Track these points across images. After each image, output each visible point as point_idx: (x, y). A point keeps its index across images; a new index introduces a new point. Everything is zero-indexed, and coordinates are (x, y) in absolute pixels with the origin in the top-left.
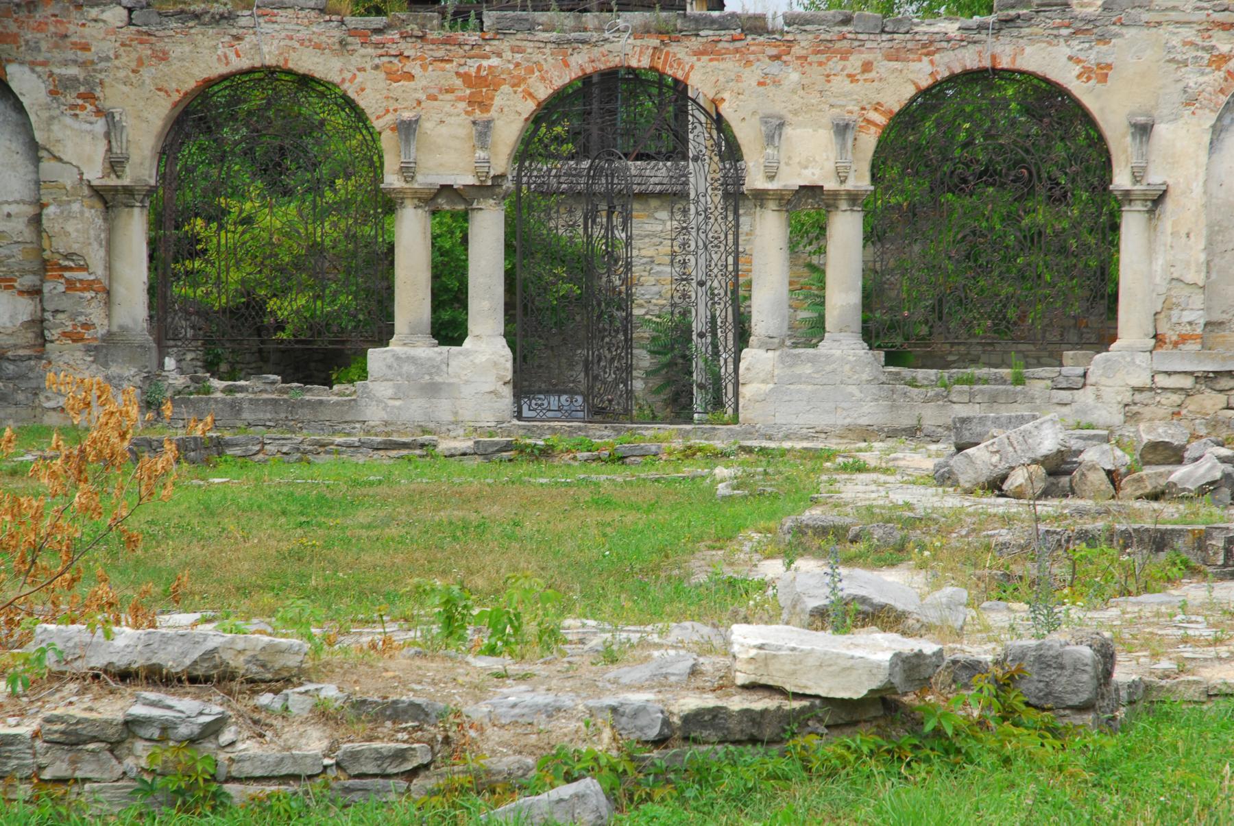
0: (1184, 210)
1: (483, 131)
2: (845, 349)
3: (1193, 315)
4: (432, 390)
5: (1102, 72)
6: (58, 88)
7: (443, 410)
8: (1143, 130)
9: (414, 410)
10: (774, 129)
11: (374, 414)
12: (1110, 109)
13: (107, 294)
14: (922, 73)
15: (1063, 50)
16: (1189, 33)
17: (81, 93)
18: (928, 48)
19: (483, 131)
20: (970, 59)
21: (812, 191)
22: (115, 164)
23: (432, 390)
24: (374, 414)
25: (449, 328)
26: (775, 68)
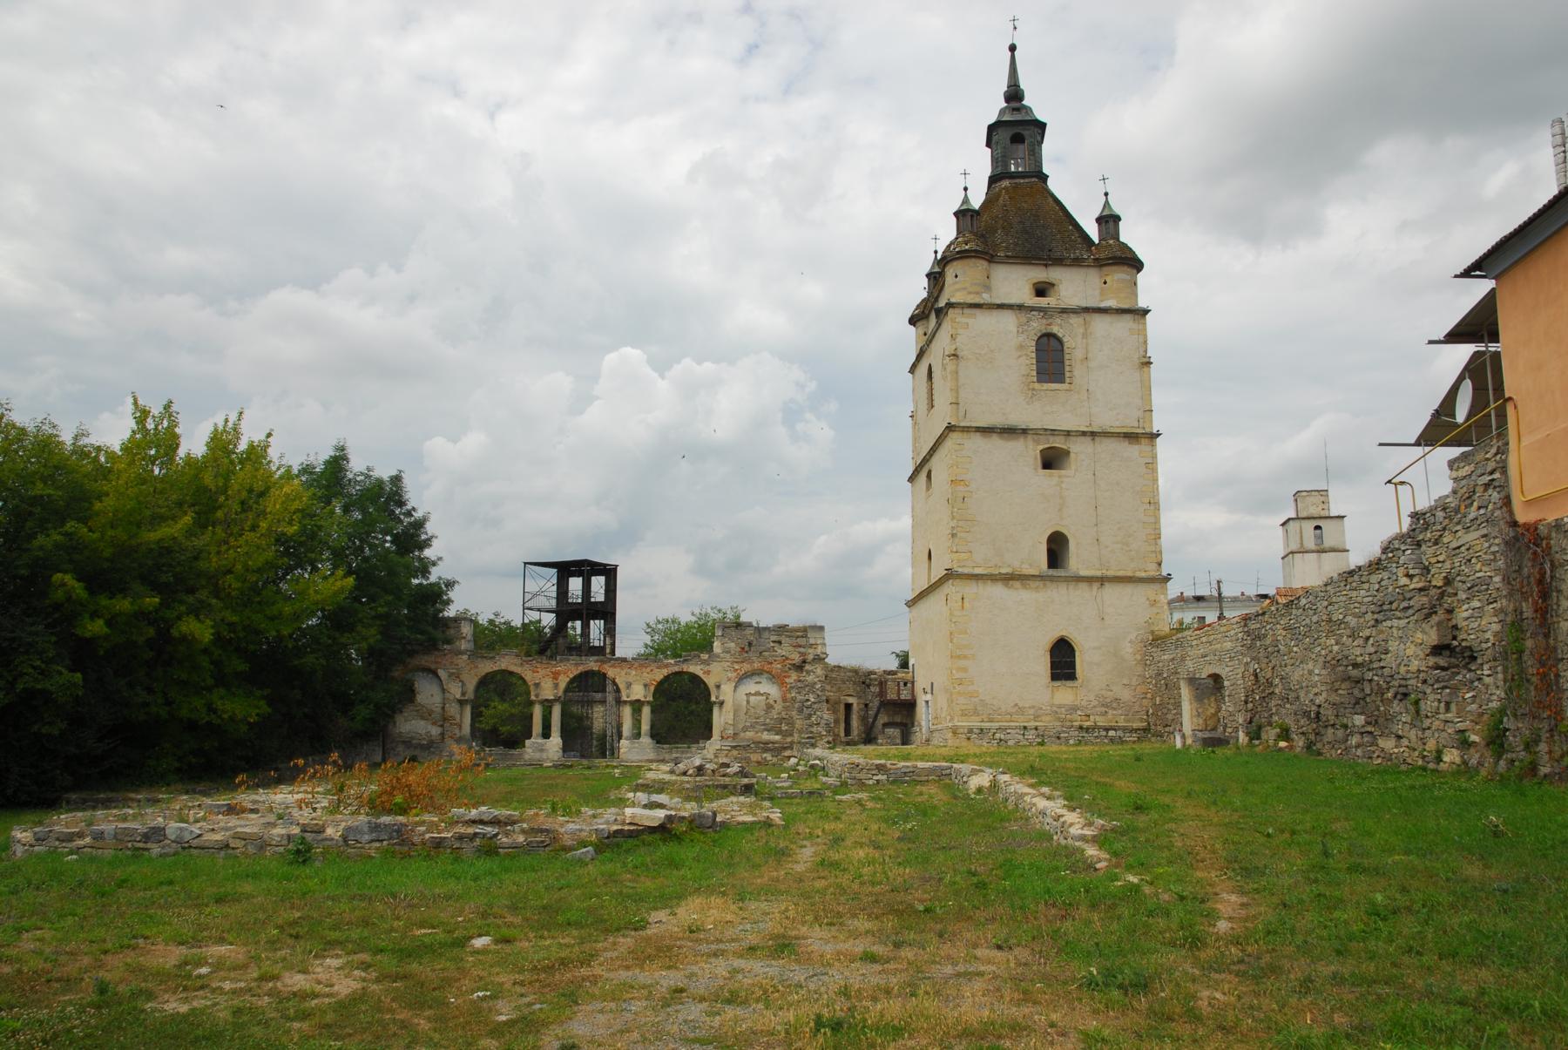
0: (728, 706)
1: (556, 686)
2: (646, 740)
3: (731, 732)
4: (542, 750)
5: (708, 672)
6: (451, 675)
7: (544, 756)
8: (718, 687)
9: (538, 755)
10: (629, 685)
11: (527, 757)
12: (710, 681)
13: (460, 727)
14: (665, 672)
17: (456, 676)
18: (667, 666)
19: (556, 686)
20: (676, 669)
21: (638, 701)
22: (463, 694)
23: (542, 750)
24: (527, 757)
25: (546, 734)
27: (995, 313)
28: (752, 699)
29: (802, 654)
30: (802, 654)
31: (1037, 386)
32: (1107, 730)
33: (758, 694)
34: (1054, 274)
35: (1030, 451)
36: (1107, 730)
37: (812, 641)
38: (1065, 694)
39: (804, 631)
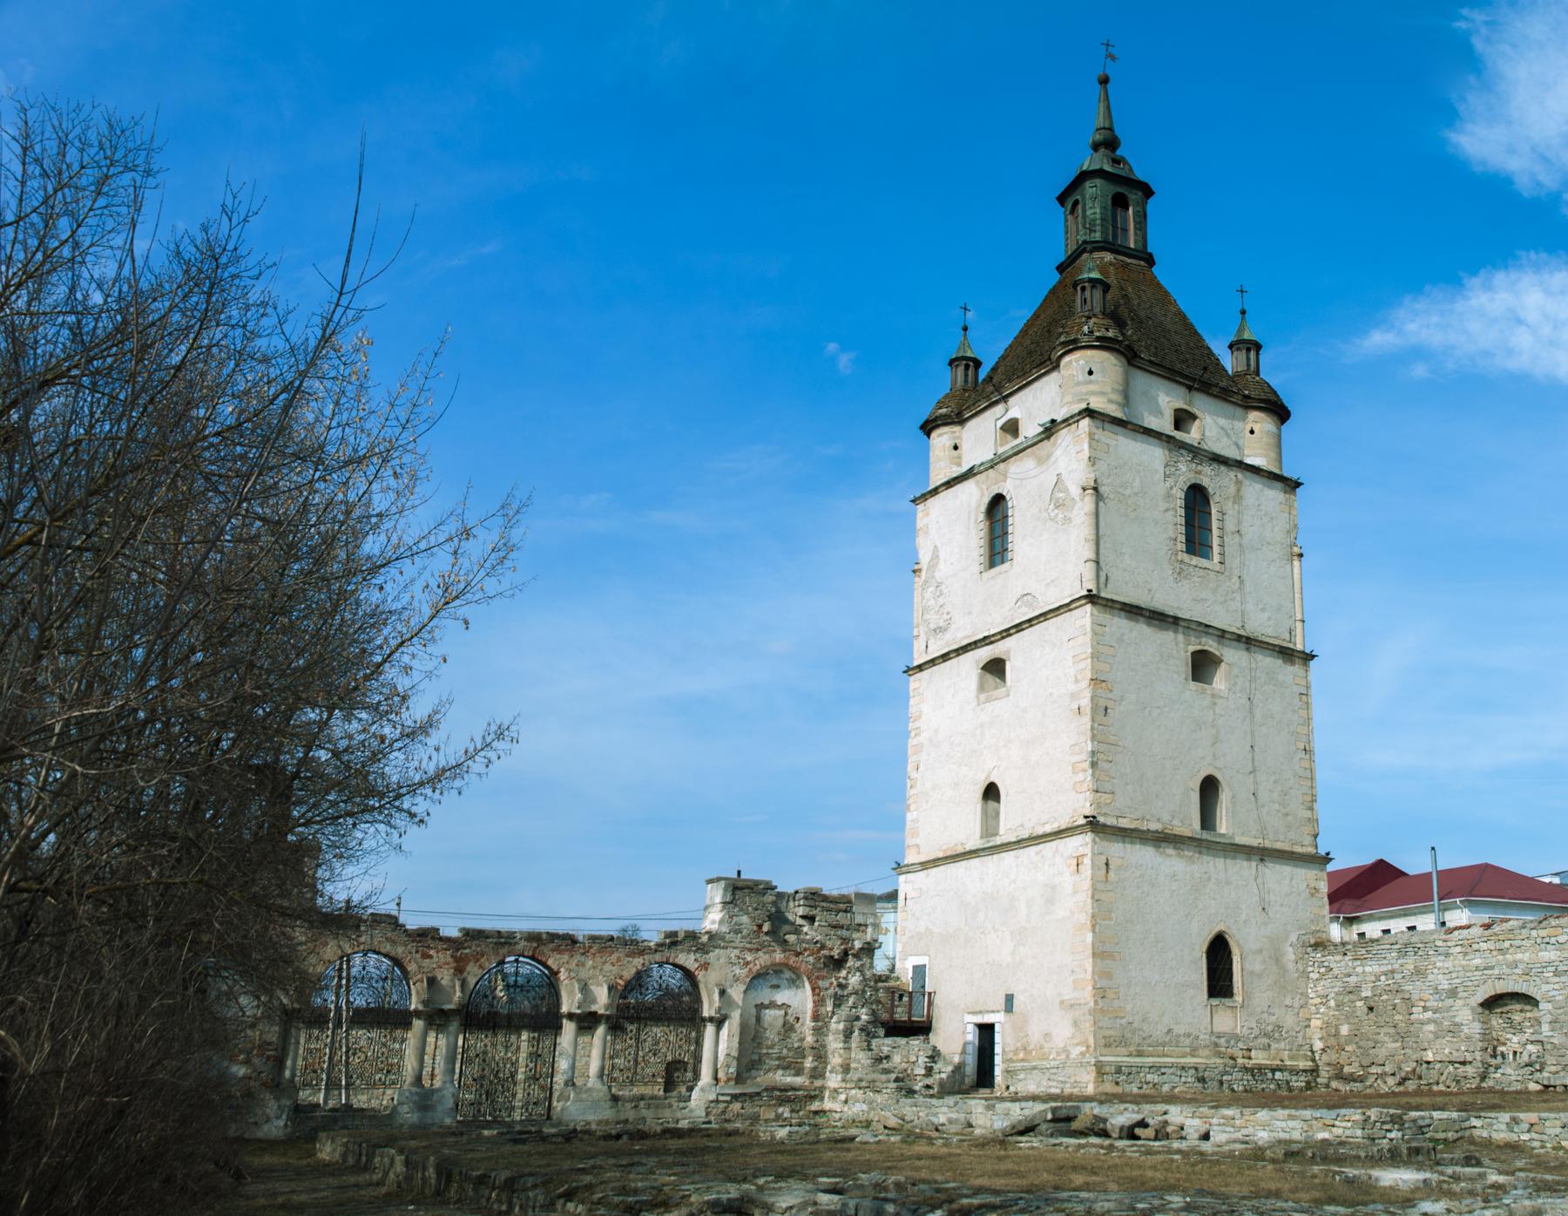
5: (705, 966)
15: (692, 957)
16: (736, 952)
26: (583, 959)
29: (845, 940)
30: (845, 940)
31: (1186, 557)
32: (1273, 1071)
35: (1177, 648)
36: (1273, 1071)
37: (859, 919)
38: (1226, 1019)
39: (843, 904)
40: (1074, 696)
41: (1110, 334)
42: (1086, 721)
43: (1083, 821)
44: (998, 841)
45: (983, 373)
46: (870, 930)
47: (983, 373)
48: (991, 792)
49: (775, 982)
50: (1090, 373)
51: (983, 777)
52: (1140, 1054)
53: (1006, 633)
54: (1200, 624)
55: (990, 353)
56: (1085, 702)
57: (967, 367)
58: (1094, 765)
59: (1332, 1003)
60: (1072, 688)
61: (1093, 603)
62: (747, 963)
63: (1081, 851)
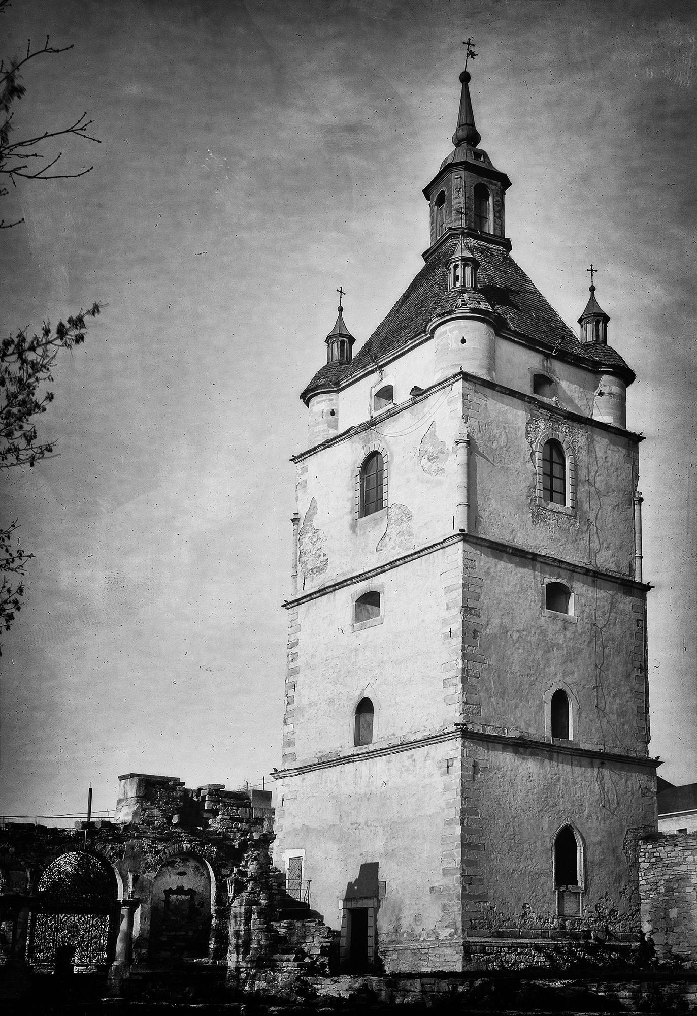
16: (148, 842)
27: (507, 399)
28: (173, 897)
33: (180, 890)
34: (559, 369)
35: (533, 582)
37: (257, 814)
40: (445, 622)
41: (482, 306)
42: (457, 642)
43: (453, 728)
44: (371, 747)
45: (357, 349)
46: (266, 823)
47: (357, 349)
48: (365, 707)
49: (181, 869)
50: (463, 341)
51: (358, 693)
52: (500, 935)
53: (382, 570)
54: (555, 560)
55: (363, 331)
56: (457, 627)
57: (343, 342)
58: (464, 680)
59: (662, 890)
60: (445, 614)
61: (464, 540)
62: (157, 852)
63: (452, 754)
